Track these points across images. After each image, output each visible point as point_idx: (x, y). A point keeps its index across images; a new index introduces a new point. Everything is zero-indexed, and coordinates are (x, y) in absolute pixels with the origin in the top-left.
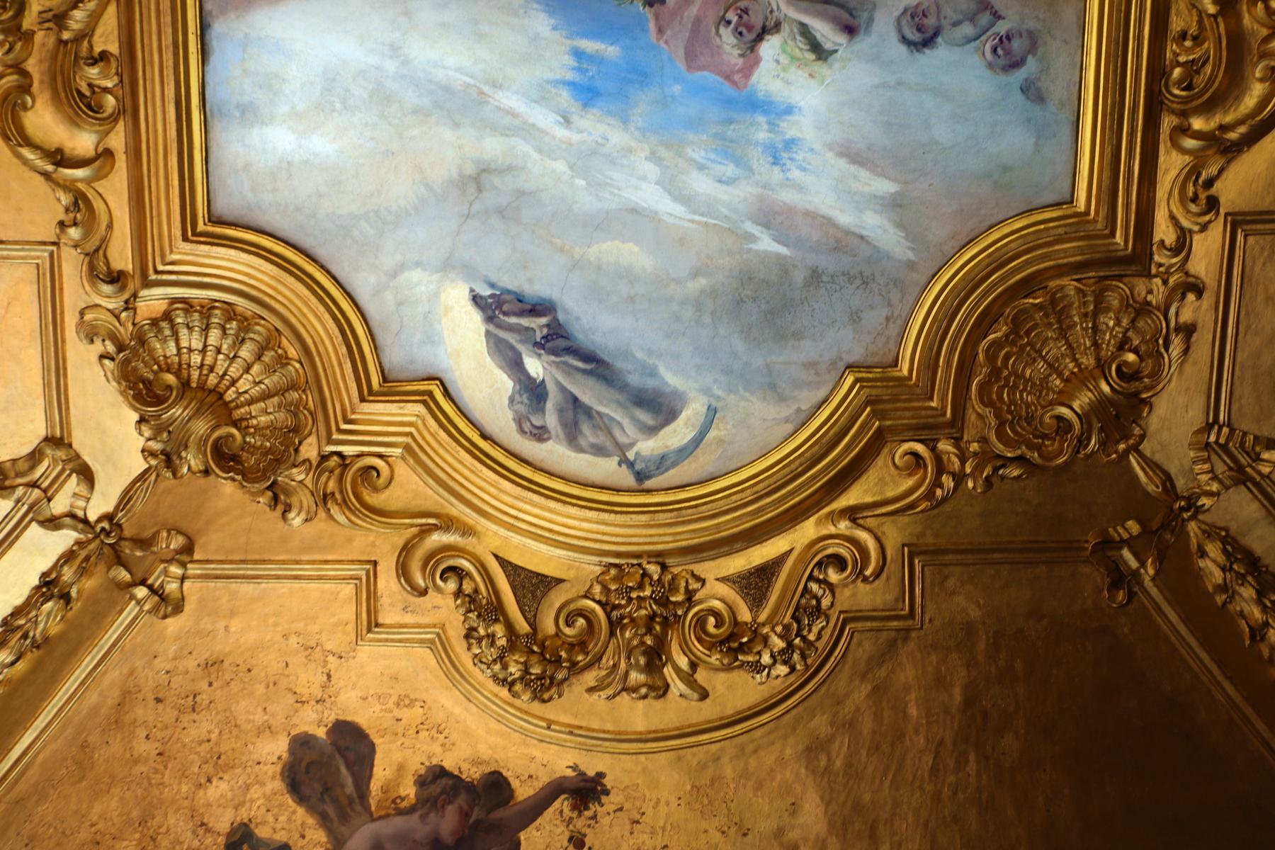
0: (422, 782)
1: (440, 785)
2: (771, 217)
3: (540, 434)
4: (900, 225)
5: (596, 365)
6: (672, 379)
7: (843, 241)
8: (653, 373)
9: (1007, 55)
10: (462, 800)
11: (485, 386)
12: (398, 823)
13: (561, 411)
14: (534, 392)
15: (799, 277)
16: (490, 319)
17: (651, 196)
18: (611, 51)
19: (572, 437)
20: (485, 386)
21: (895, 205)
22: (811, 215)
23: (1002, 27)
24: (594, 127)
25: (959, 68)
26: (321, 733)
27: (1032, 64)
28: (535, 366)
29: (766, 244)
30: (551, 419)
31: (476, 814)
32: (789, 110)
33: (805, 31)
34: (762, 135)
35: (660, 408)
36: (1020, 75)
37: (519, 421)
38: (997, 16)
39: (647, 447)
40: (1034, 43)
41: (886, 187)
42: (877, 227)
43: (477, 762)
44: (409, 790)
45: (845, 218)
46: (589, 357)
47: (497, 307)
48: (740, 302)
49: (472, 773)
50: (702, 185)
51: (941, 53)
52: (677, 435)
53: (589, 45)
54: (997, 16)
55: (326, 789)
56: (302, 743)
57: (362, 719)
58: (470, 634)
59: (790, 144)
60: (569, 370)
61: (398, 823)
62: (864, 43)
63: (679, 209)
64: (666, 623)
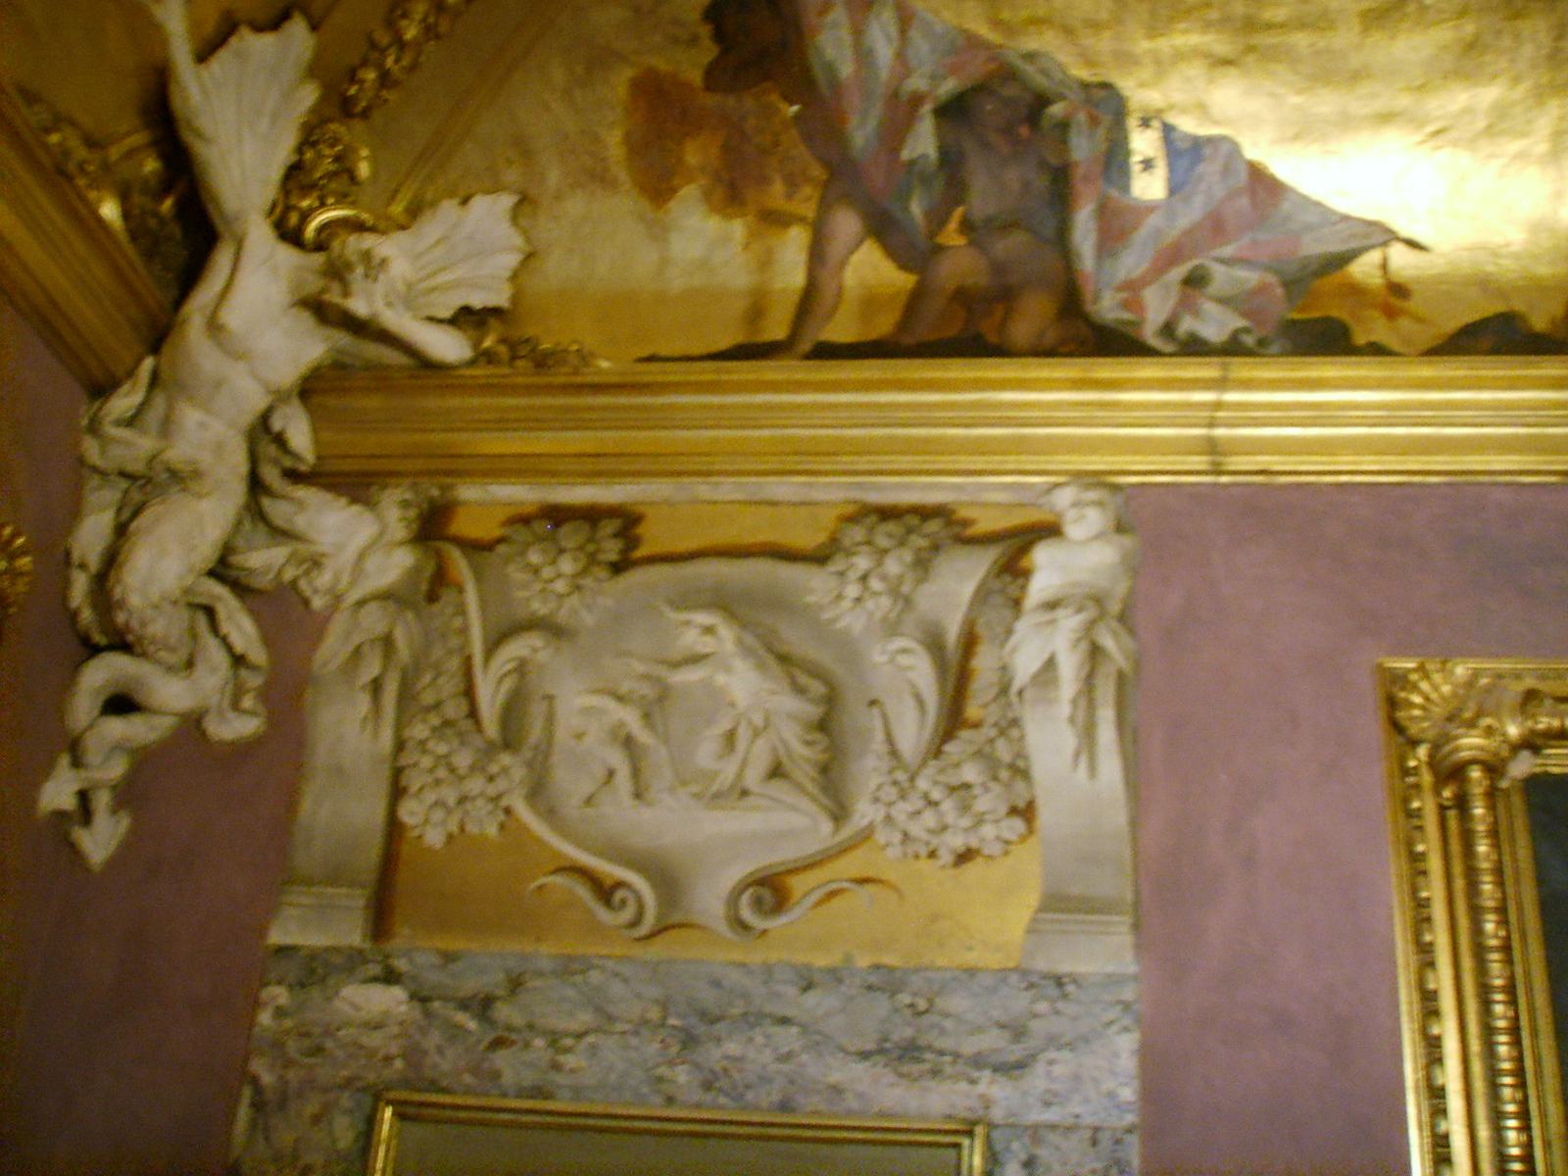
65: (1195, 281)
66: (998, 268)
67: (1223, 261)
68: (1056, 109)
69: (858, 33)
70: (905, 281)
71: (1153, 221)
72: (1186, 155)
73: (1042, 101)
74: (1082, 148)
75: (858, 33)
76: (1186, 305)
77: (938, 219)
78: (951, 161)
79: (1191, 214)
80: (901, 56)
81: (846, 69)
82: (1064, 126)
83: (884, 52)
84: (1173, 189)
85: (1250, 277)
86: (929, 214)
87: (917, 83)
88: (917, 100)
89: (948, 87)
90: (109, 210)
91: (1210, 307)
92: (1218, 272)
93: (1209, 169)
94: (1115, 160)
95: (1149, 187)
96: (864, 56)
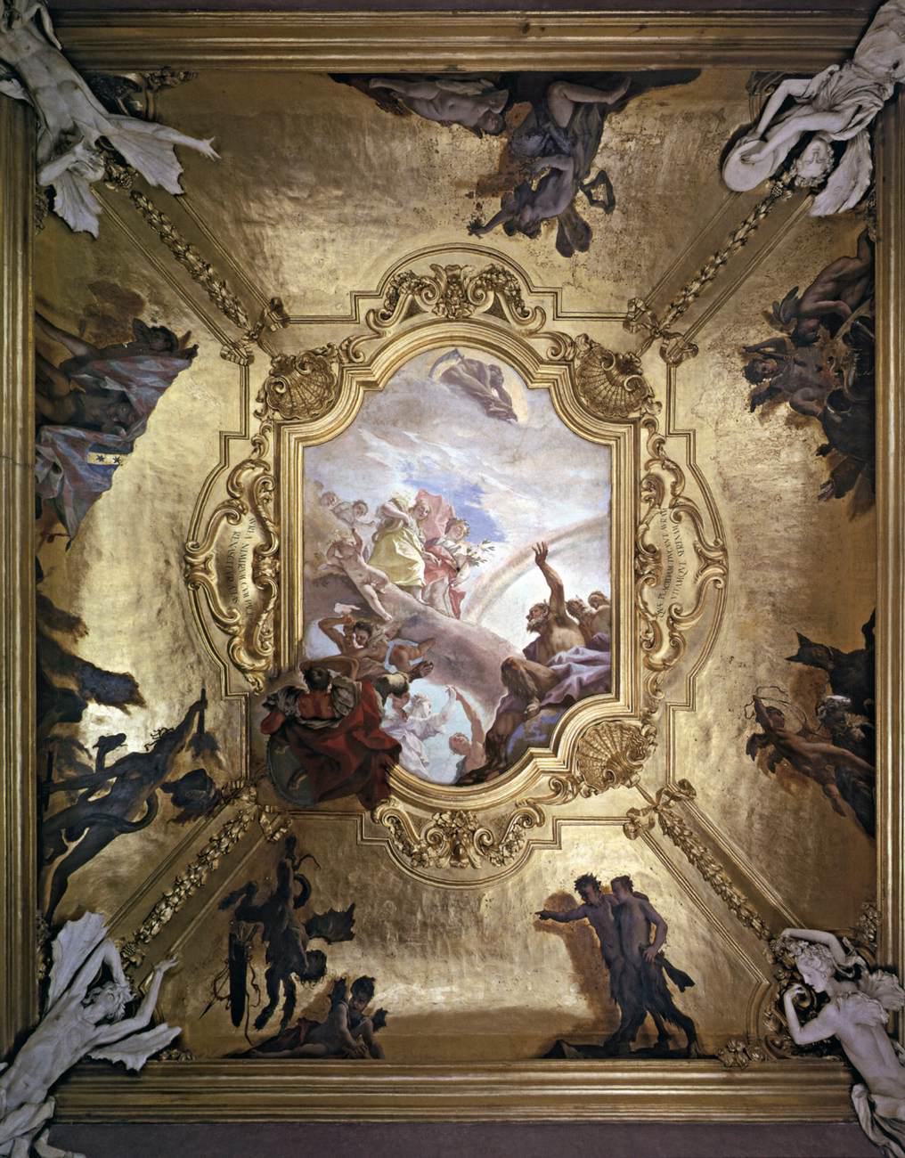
0: (538, 231)
1: (532, 232)
2: (412, 444)
3: (493, 368)
4: (364, 441)
5: (472, 393)
6: (445, 387)
7: (384, 436)
8: (452, 390)
9: (330, 497)
10: (523, 224)
11: (512, 384)
12: (548, 214)
13: (485, 377)
14: (496, 383)
15: (400, 424)
16: (511, 410)
17: (453, 453)
18: (467, 503)
19: (481, 365)
20: (512, 384)
21: (367, 448)
22: (397, 445)
23: (331, 507)
24: (474, 478)
25: (347, 495)
26: (576, 252)
27: (320, 495)
28: (495, 393)
29: (412, 435)
30: (489, 373)
31: (517, 219)
32: (405, 482)
33: (400, 509)
34: (414, 473)
35: (449, 377)
36: (324, 491)
37: (500, 373)
38: (333, 511)
39: (453, 363)
40: (320, 502)
41: (370, 455)
42: (374, 442)
43: (517, 240)
44: (543, 228)
45: (384, 443)
46: (475, 396)
47: (509, 415)
48: (421, 415)
49: (519, 236)
50: (436, 457)
51: (352, 499)
52: (443, 367)
53: (475, 505)
54: (333, 511)
55: (575, 229)
56: (584, 248)
57: (558, 258)
58: (518, 291)
59: (404, 470)
60: (482, 391)
61: (548, 214)
62: (378, 504)
63: (444, 449)
64: (446, 295)
65: (56, 468)
66: (61, 399)
67: (63, 479)
68: (123, 431)
69: (154, 373)
70: (57, 363)
71: (79, 457)
72: (107, 471)
73: (127, 428)
74: (108, 438)
75: (154, 373)
76: (47, 463)
77: (81, 382)
78: (106, 393)
79: (83, 472)
80: (145, 385)
81: (141, 367)
82: (117, 433)
83: (148, 380)
84: (90, 465)
85: (57, 487)
86: (83, 379)
87: (135, 388)
88: (128, 387)
89: (133, 399)
90: (132, 76)
91: (46, 470)
92: (59, 477)
93: (99, 479)
94: (103, 448)
95: (93, 458)
96: (147, 373)
